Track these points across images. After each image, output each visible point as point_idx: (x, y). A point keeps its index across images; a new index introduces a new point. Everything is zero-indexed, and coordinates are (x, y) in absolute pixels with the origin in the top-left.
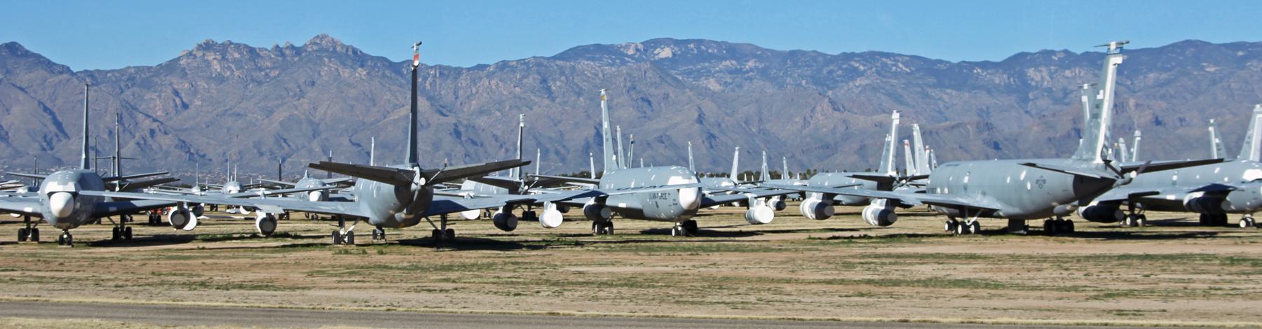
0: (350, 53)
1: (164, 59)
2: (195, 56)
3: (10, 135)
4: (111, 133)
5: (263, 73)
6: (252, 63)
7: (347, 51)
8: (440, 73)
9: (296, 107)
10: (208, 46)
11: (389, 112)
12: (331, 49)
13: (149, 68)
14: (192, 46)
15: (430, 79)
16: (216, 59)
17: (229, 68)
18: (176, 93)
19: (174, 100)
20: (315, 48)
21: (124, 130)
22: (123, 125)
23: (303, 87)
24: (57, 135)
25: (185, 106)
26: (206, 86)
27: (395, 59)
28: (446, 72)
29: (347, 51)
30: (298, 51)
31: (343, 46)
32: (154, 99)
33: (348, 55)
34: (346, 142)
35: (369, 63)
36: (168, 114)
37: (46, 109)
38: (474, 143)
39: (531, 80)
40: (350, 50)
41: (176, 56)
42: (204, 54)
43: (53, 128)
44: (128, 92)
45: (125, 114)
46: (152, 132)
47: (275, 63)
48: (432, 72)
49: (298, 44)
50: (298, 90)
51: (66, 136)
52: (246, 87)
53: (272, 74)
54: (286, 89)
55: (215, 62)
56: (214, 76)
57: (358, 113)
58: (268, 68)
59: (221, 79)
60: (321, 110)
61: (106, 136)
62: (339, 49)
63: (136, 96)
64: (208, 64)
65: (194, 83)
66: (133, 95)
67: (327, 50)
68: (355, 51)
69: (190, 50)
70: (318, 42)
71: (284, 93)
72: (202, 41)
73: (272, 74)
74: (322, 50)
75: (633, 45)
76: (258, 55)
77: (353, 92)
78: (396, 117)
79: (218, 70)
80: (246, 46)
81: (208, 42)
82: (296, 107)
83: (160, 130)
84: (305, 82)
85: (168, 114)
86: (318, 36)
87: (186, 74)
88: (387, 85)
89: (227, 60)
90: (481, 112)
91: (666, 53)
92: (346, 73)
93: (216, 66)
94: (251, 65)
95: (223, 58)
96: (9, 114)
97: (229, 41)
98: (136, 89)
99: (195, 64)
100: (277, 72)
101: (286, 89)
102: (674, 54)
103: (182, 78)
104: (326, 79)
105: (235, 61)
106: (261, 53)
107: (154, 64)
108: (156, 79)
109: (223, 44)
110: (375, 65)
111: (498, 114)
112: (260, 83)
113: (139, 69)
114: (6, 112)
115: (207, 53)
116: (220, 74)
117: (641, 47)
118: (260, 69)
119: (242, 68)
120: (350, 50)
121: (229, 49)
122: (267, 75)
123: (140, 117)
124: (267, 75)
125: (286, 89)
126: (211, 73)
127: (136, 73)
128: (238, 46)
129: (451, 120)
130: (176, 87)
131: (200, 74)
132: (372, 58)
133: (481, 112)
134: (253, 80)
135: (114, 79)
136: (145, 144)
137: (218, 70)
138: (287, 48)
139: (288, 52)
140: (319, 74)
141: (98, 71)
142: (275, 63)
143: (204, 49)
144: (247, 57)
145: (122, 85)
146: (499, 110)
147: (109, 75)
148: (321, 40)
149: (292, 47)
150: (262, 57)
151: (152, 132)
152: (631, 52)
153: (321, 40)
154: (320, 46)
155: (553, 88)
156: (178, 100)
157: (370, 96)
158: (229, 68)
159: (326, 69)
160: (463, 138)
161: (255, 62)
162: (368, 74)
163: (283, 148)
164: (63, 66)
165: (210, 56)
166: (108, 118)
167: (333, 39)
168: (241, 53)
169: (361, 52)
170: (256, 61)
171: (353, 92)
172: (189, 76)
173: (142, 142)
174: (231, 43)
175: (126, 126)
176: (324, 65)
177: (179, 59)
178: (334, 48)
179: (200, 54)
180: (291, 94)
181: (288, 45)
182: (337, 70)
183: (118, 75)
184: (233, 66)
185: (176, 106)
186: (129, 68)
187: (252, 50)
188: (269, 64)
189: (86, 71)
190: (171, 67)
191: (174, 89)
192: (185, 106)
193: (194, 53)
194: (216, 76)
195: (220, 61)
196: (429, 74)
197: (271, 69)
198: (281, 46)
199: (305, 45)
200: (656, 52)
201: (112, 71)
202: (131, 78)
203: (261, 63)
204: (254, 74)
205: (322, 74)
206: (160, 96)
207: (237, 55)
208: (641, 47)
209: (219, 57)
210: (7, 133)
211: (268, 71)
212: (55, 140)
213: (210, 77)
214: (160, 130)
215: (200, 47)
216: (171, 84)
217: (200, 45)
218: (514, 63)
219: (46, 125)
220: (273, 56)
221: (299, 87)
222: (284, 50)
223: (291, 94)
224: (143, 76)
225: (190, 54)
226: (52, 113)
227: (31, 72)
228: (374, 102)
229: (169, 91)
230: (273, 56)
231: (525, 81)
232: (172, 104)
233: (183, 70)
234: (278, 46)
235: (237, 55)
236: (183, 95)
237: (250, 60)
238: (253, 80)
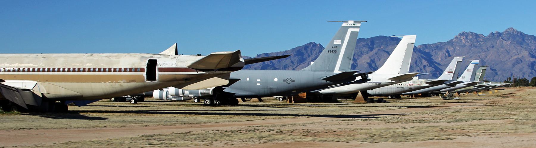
0: (519, 34)
1: (448, 40)
2: (458, 38)
5: (478, 43)
6: (476, 40)
7: (518, 33)
10: (463, 34)
12: (512, 33)
13: (445, 42)
14: (457, 34)
16: (464, 38)
17: (468, 42)
18: (448, 52)
19: (446, 54)
20: (506, 33)
21: (416, 66)
22: (417, 64)
23: (489, 48)
25: (450, 56)
29: (518, 33)
30: (500, 34)
31: (517, 31)
32: (440, 54)
33: (518, 35)
35: (526, 38)
36: (442, 59)
40: (519, 33)
41: (453, 38)
42: (461, 37)
44: (434, 52)
45: (418, 60)
46: (425, 67)
47: (484, 39)
50: (486, 49)
53: (481, 44)
54: (482, 49)
55: (463, 40)
56: (462, 45)
57: (501, 58)
58: (481, 41)
59: (464, 46)
62: (514, 33)
63: (436, 53)
65: (455, 48)
66: (435, 53)
67: (510, 34)
68: (521, 33)
70: (508, 30)
71: (481, 51)
72: (461, 32)
73: (481, 44)
74: (509, 33)
76: (479, 37)
79: (464, 43)
80: (475, 33)
81: (463, 32)
83: (428, 66)
84: (490, 46)
85: (442, 59)
87: (453, 44)
88: (517, 47)
89: (468, 39)
95: (466, 38)
96: (380, 61)
97: (470, 32)
98: (436, 50)
99: (457, 41)
100: (483, 43)
101: (482, 49)
103: (451, 46)
105: (471, 39)
107: (446, 41)
108: (444, 47)
110: (528, 38)
112: (476, 47)
114: (379, 60)
115: (461, 37)
116: (464, 44)
118: (478, 42)
120: (519, 33)
121: (469, 35)
122: (480, 44)
124: (480, 44)
125: (482, 49)
126: (461, 44)
127: (440, 44)
130: (449, 49)
131: (458, 44)
132: (528, 36)
134: (474, 46)
135: (432, 47)
136: (421, 71)
137: (464, 43)
138: (496, 33)
140: (496, 43)
142: (484, 39)
147: (431, 45)
148: (509, 30)
149: (498, 33)
153: (509, 30)
154: (508, 32)
156: (447, 54)
157: (508, 51)
158: (468, 42)
159: (499, 41)
161: (477, 39)
162: (511, 43)
167: (514, 29)
168: (473, 36)
169: (524, 34)
170: (478, 39)
172: (454, 45)
173: (420, 70)
174: (470, 32)
175: (418, 64)
176: (499, 40)
177: (453, 39)
178: (513, 33)
179: (459, 37)
180: (484, 51)
181: (496, 32)
182: (502, 41)
183: (434, 45)
184: (469, 42)
185: (446, 56)
186: (438, 42)
187: (477, 35)
188: (481, 40)
189: (424, 44)
190: (451, 42)
191: (447, 50)
193: (458, 37)
194: (463, 45)
195: (465, 40)
198: (494, 33)
199: (504, 32)
201: (432, 44)
203: (479, 39)
204: (475, 44)
205: (497, 43)
207: (471, 37)
209: (465, 38)
211: (480, 42)
213: (461, 46)
214: (428, 66)
215: (460, 35)
217: (460, 34)
220: (484, 37)
221: (487, 48)
222: (495, 34)
223: (484, 51)
224: (442, 46)
225: (457, 37)
227: (392, 46)
229: (444, 51)
230: (484, 37)
232: (444, 56)
233: (453, 43)
234: (492, 33)
235: (471, 37)
236: (450, 52)
237: (475, 39)
238: (474, 46)
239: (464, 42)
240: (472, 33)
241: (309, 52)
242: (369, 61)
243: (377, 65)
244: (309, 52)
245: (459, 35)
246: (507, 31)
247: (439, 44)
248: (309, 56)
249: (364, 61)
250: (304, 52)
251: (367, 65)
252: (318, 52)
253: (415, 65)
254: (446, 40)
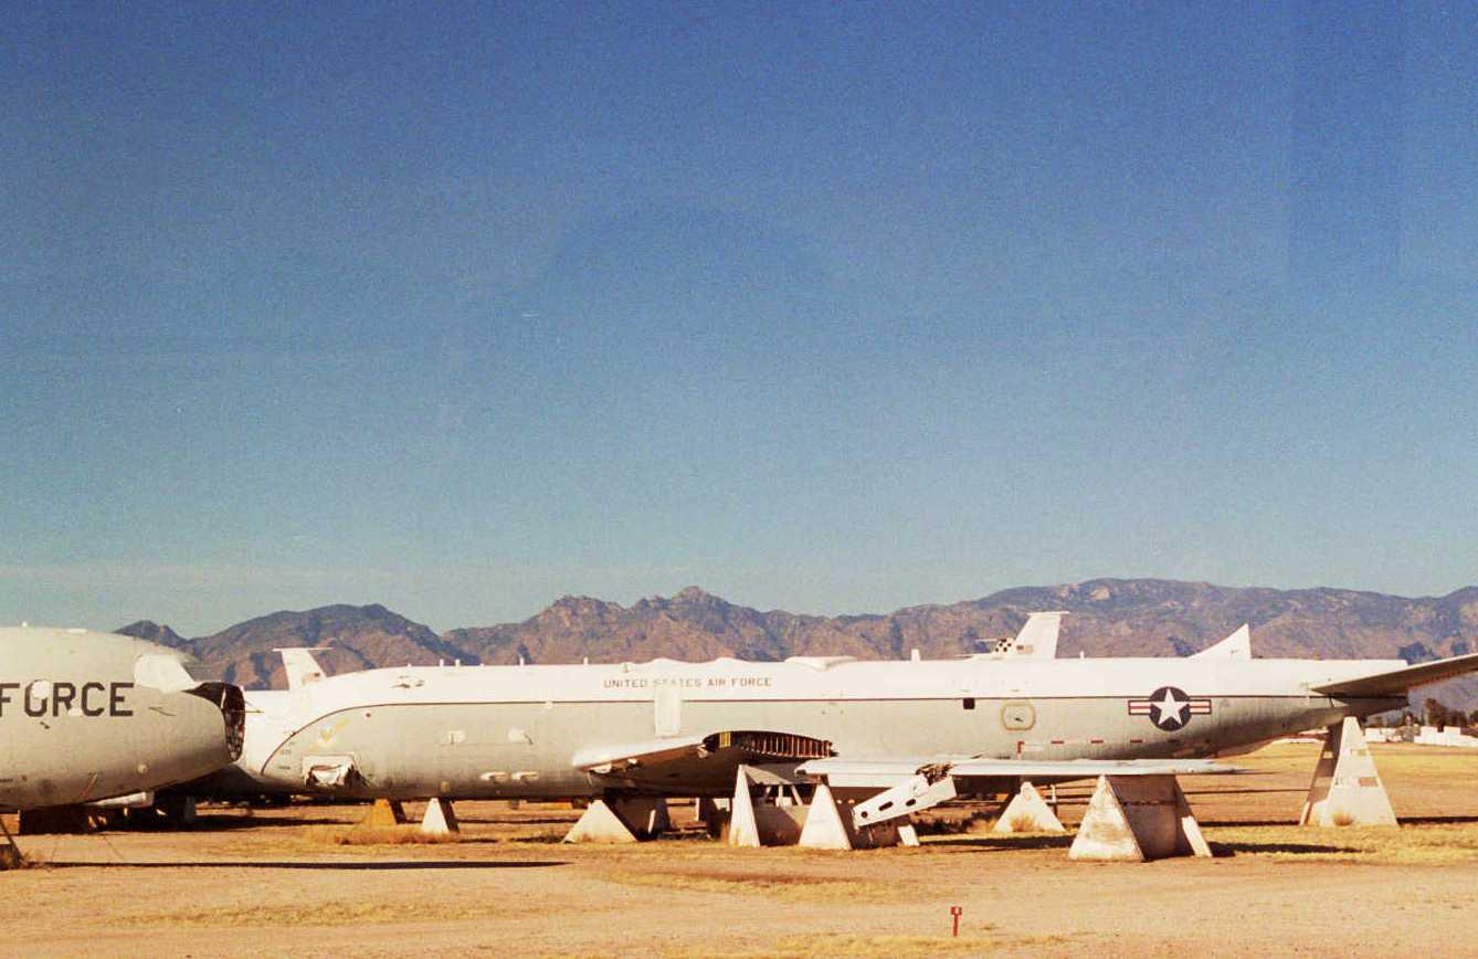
0: (713, 604)
10: (565, 602)
14: (550, 602)
17: (577, 624)
28: (806, 621)
30: (663, 604)
31: (708, 596)
39: (883, 630)
49: (666, 596)
59: (569, 634)
64: (560, 620)
75: (1066, 588)
80: (597, 601)
91: (1103, 594)
95: (574, 614)
102: (1111, 594)
106: (610, 607)
117: (1076, 588)
118: (603, 623)
130: (525, 643)
138: (653, 601)
150: (610, 612)
152: (1064, 594)
155: (905, 636)
165: (563, 613)
168: (591, 608)
174: (585, 598)
177: (538, 616)
178: (697, 600)
188: (614, 619)
198: (648, 599)
199: (674, 598)
200: (1092, 594)
201: (482, 630)
208: (1076, 588)
209: (570, 613)
215: (557, 603)
235: (586, 610)
236: (530, 651)
239: (568, 624)
245: (555, 605)
246: (682, 596)
247: (500, 628)
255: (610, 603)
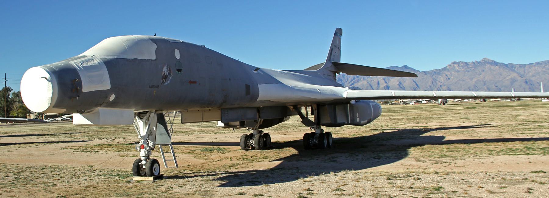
0: (493, 62)
1: (443, 67)
2: (451, 66)
3: (405, 88)
4: (430, 86)
7: (492, 62)
8: (520, 66)
9: (479, 77)
10: (454, 63)
11: (505, 77)
12: (488, 62)
13: (439, 69)
14: (450, 63)
15: (517, 68)
17: (460, 68)
18: (447, 76)
19: (446, 77)
20: (483, 61)
24: (417, 88)
25: (449, 79)
26: (454, 73)
27: (506, 63)
29: (492, 62)
30: (478, 63)
31: (491, 60)
34: (494, 86)
37: (414, 81)
38: (531, 85)
41: (446, 66)
42: (453, 65)
43: (416, 86)
45: (434, 82)
48: (517, 66)
49: (478, 61)
51: (419, 88)
52: (465, 73)
55: (457, 67)
58: (471, 68)
59: (458, 71)
60: (486, 78)
61: (429, 87)
62: (490, 61)
64: (455, 67)
68: (495, 62)
69: (450, 64)
72: (453, 62)
73: (472, 69)
74: (485, 62)
76: (468, 65)
77: (495, 72)
78: (508, 79)
80: (465, 62)
82: (479, 77)
86: (484, 59)
89: (460, 66)
90: (533, 76)
92: (492, 67)
93: (457, 68)
94: (466, 67)
95: (459, 66)
98: (436, 75)
104: (487, 69)
105: (462, 66)
107: (440, 68)
108: (441, 72)
109: (458, 62)
111: (538, 76)
113: (437, 70)
115: (454, 65)
116: (458, 70)
118: (469, 68)
119: (464, 68)
122: (471, 69)
123: (438, 82)
124: (471, 69)
127: (436, 71)
128: (462, 62)
129: (524, 78)
130: (446, 74)
132: (500, 63)
133: (533, 76)
134: (467, 71)
138: (476, 62)
139: (476, 63)
140: (485, 68)
141: (426, 71)
143: (453, 64)
144: (465, 65)
145: (433, 74)
146: (538, 75)
149: (477, 62)
151: (441, 86)
158: (460, 68)
160: (528, 83)
163: (476, 88)
164: (418, 70)
165: (455, 65)
166: (429, 83)
168: (463, 64)
171: (495, 72)
173: (438, 88)
177: (447, 67)
178: (489, 61)
179: (452, 65)
182: (490, 67)
183: (431, 72)
184: (461, 67)
186: (434, 70)
187: (466, 63)
188: (471, 66)
190: (445, 69)
192: (449, 79)
193: (451, 65)
195: (458, 67)
196: (516, 67)
197: (472, 68)
199: (481, 61)
202: (435, 72)
204: (467, 69)
206: (442, 77)
207: (462, 65)
209: (457, 65)
210: (405, 88)
212: (416, 89)
213: (455, 71)
215: (452, 63)
216: (445, 73)
217: (452, 63)
218: (541, 62)
219: (414, 85)
221: (479, 72)
223: (477, 74)
224: (438, 72)
225: (450, 65)
226: (415, 82)
228: (501, 75)
230: (472, 64)
231: (546, 67)
232: (445, 78)
233: (448, 69)
235: (462, 65)
236: (448, 76)
238: (467, 71)
240: (462, 62)
241: (346, 79)
242: (398, 83)
243: (404, 85)
244: (346, 79)
246: (483, 60)
247: (435, 70)
248: (346, 82)
249: (394, 83)
250: (342, 79)
251: (398, 86)
252: (352, 79)
253: (432, 85)
254: (440, 67)
255: (469, 63)
